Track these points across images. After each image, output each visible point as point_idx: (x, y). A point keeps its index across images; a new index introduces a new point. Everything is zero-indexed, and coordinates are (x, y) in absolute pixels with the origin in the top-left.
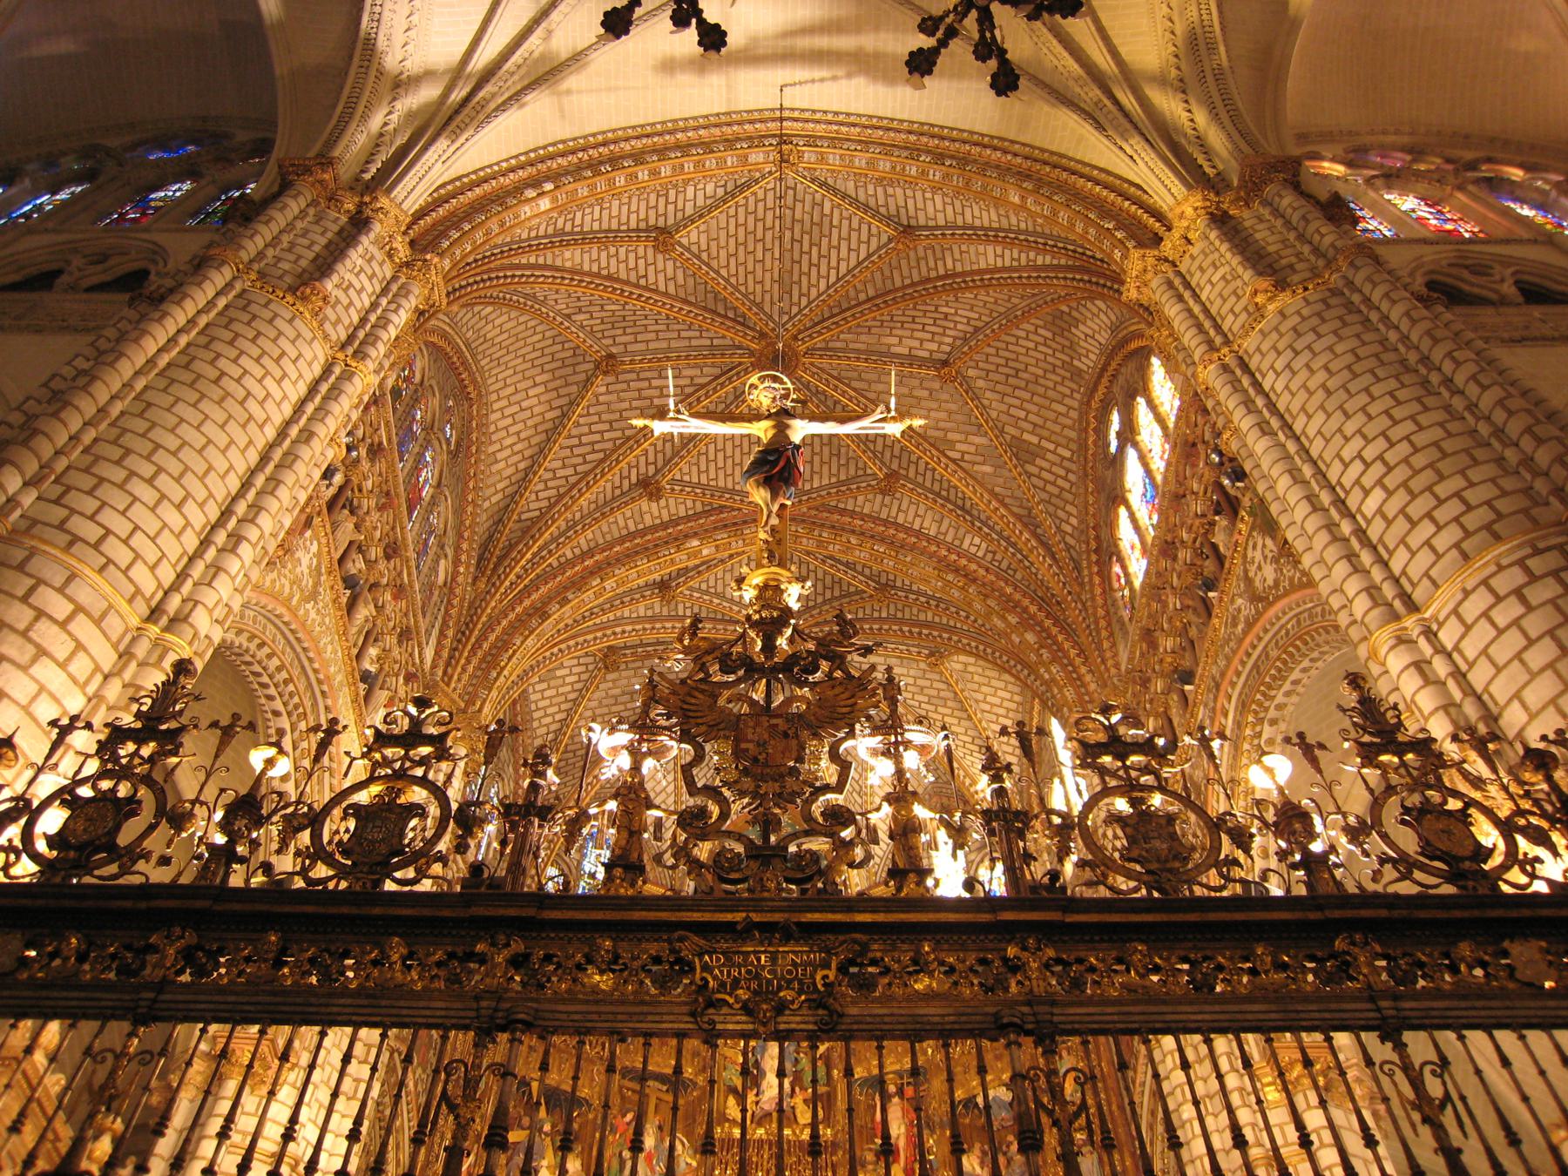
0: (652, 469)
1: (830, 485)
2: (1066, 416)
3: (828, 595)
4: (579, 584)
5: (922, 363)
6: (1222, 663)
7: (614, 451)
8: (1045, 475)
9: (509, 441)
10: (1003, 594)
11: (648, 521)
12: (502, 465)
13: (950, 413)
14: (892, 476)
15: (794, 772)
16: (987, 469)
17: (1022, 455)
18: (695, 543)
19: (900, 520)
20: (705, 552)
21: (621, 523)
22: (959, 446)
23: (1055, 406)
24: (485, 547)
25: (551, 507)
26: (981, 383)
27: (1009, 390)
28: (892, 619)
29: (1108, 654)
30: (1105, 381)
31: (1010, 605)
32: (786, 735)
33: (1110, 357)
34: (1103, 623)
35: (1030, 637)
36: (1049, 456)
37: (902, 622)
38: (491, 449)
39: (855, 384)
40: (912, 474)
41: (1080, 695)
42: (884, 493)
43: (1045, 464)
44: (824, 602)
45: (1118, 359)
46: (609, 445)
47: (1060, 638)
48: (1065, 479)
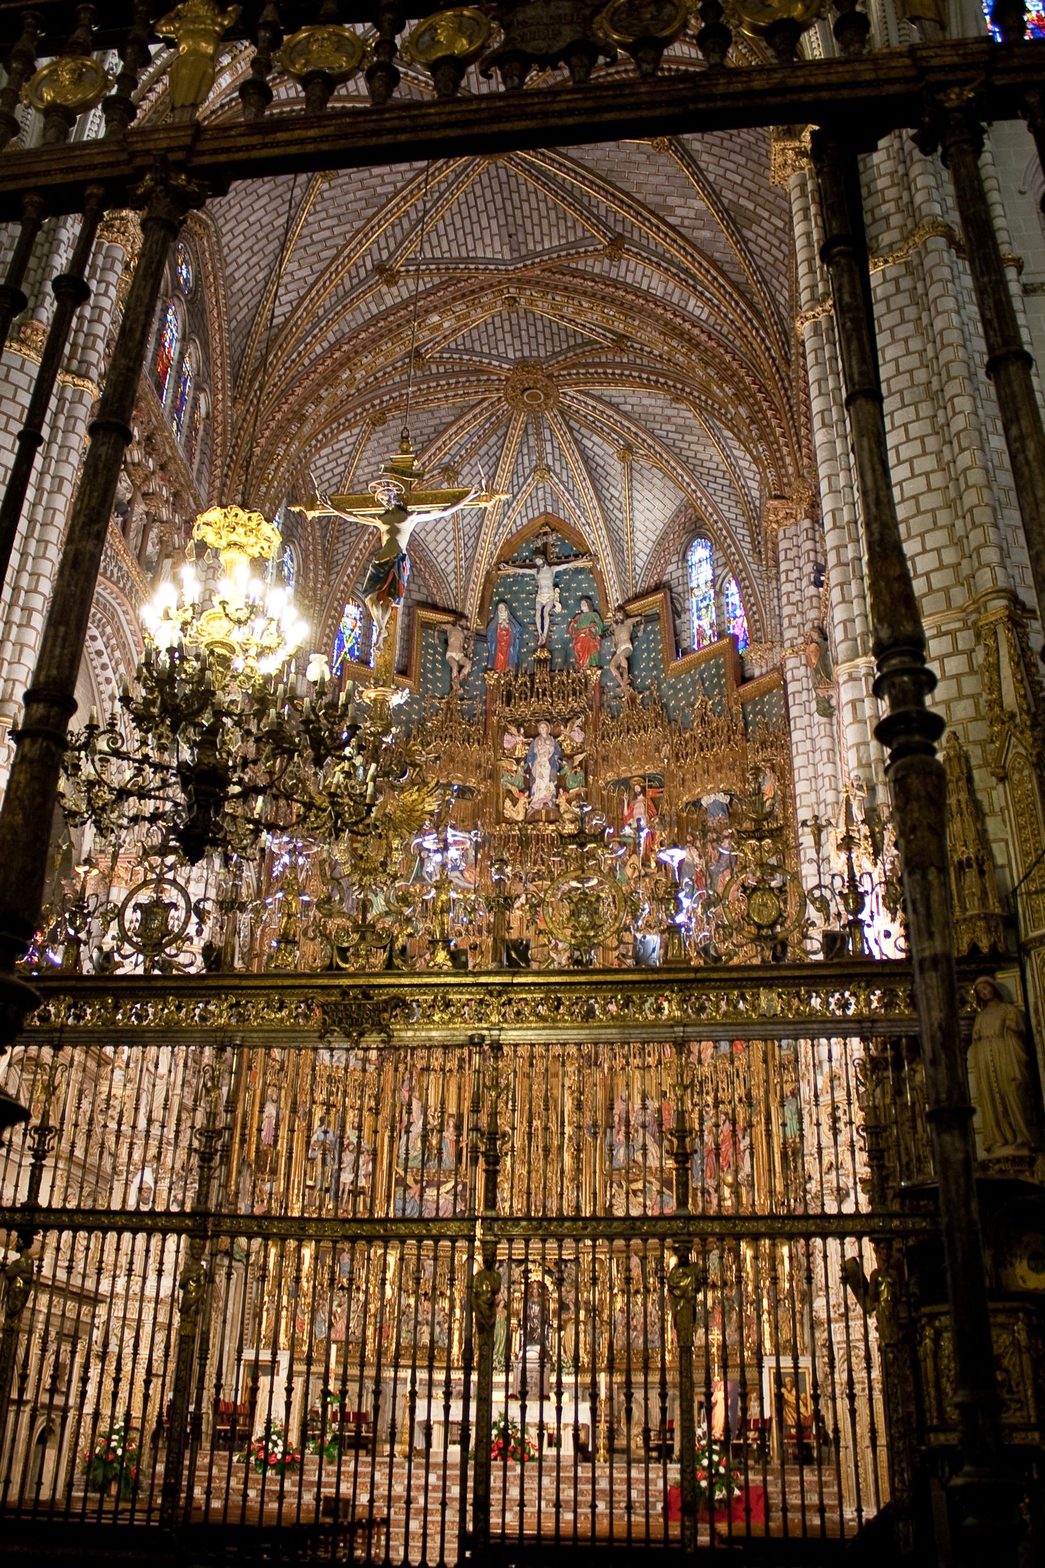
0: (385, 255)
1: (561, 248)
3: (572, 342)
4: (330, 379)
7: (346, 246)
9: (243, 258)
10: (723, 362)
11: (389, 301)
12: (241, 282)
16: (707, 234)
17: (740, 220)
18: (435, 318)
19: (629, 280)
20: (446, 325)
21: (364, 308)
22: (679, 211)
24: (237, 365)
25: (294, 311)
29: (804, 442)
31: (726, 376)
36: (764, 223)
37: (641, 369)
38: (228, 272)
40: (636, 237)
41: (779, 476)
43: (762, 233)
46: (340, 241)
48: (779, 249)
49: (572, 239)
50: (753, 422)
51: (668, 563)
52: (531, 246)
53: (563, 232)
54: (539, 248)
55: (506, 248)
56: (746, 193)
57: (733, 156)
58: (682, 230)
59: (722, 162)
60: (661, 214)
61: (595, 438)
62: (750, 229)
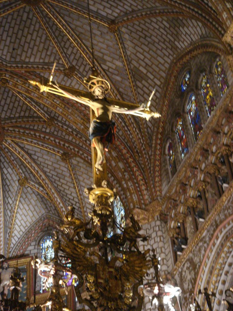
1: (39, 63)
2: (163, 65)
3: (22, 114)
5: (102, 18)
6: (222, 217)
8: (145, 89)
13: (108, 46)
14: (72, 69)
15: (121, 297)
16: (118, 78)
22: (108, 63)
23: (159, 59)
26: (126, 36)
27: (139, 44)
28: (51, 134)
30: (188, 57)
32: (116, 278)
33: (196, 48)
34: (157, 169)
35: (121, 165)
36: (149, 81)
37: (56, 137)
39: (66, 18)
40: (81, 70)
41: (140, 200)
42: (66, 75)
43: (146, 84)
44: (19, 117)
45: (200, 51)
47: (135, 169)
49: (47, 61)
50: (125, 171)
51: (29, 245)
52: (23, 58)
53: (43, 56)
54: (27, 60)
55: (9, 55)
56: (144, 64)
57: (143, 46)
58: (108, 73)
59: (137, 48)
60: (100, 62)
61: (9, 170)
62: (141, 82)
